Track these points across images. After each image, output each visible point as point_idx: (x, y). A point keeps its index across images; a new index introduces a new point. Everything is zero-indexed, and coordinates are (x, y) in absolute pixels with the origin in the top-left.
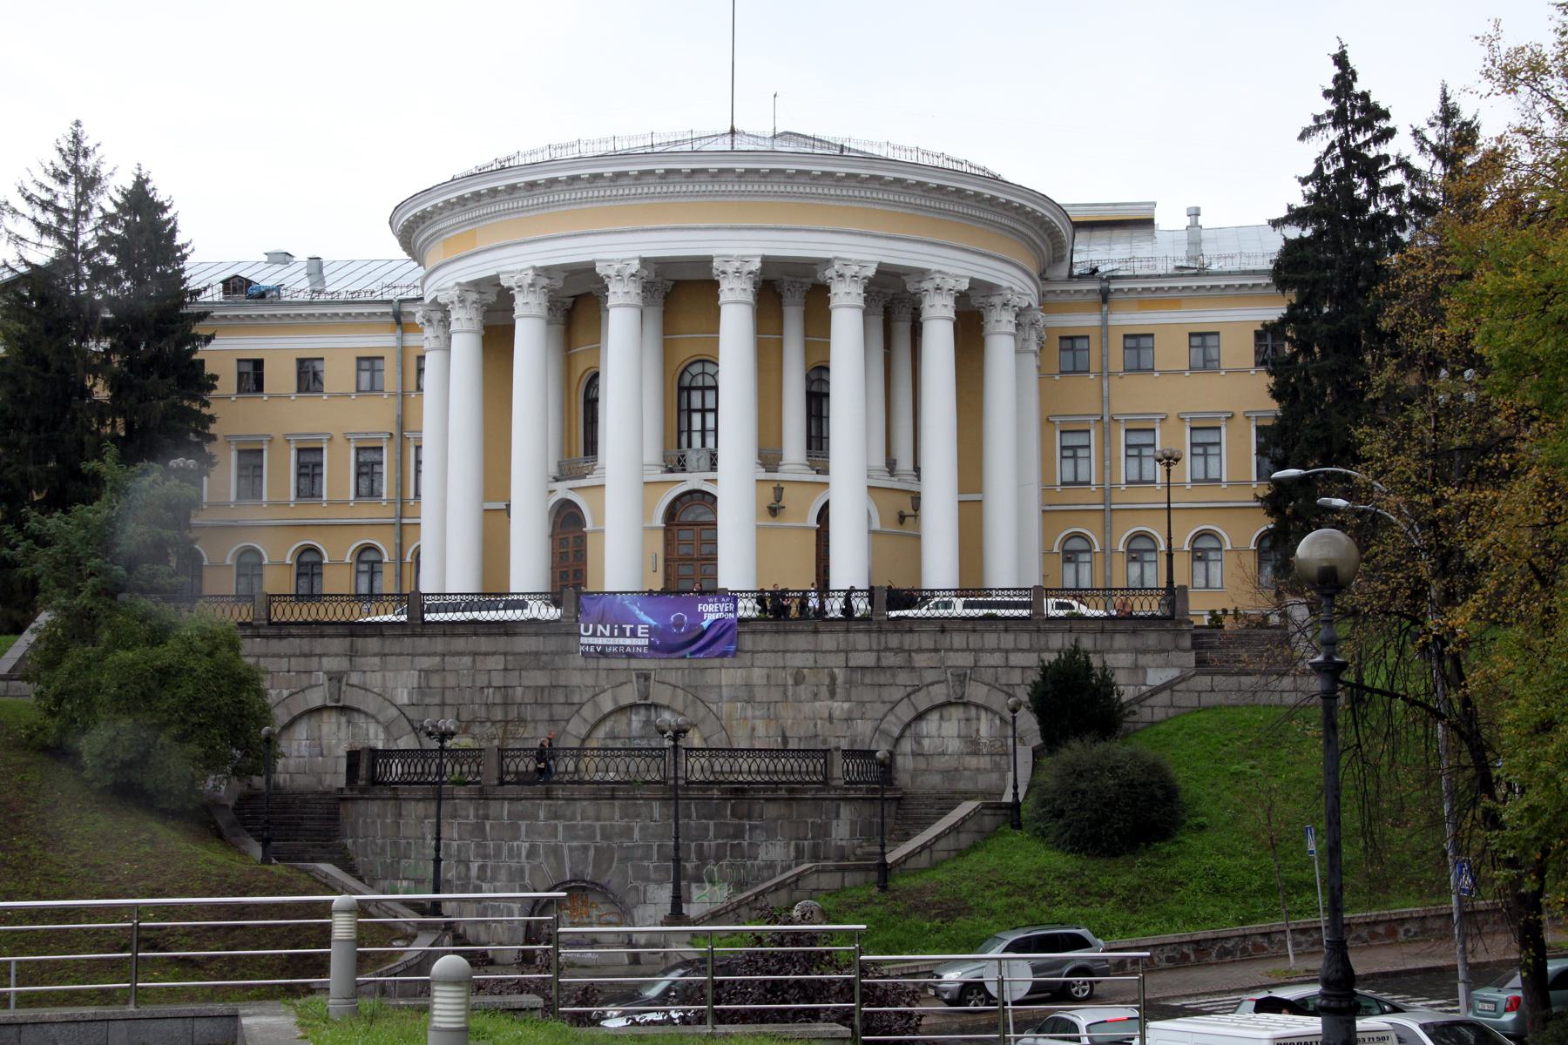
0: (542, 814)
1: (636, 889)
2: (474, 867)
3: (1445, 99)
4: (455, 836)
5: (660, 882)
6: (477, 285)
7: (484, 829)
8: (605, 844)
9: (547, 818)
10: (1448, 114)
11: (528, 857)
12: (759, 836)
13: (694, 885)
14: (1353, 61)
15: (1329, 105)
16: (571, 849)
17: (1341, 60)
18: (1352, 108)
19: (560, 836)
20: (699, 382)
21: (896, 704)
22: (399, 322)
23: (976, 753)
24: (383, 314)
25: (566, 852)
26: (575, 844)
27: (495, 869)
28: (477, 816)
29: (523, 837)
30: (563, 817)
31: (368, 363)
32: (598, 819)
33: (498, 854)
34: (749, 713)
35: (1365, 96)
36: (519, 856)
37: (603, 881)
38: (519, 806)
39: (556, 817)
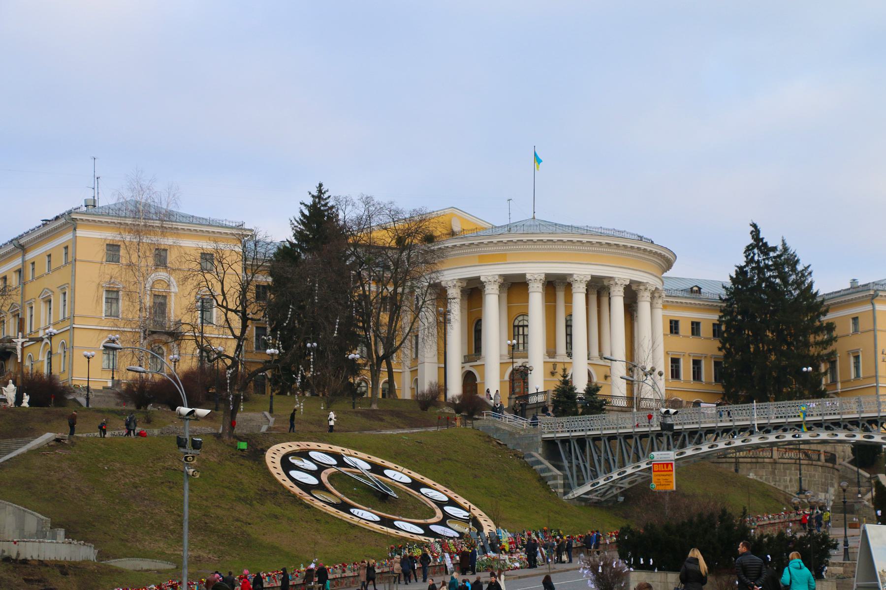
3: (784, 244)
6: (500, 276)
15: (752, 241)
17: (754, 226)
18: (758, 243)
35: (762, 239)
38: (786, 466)
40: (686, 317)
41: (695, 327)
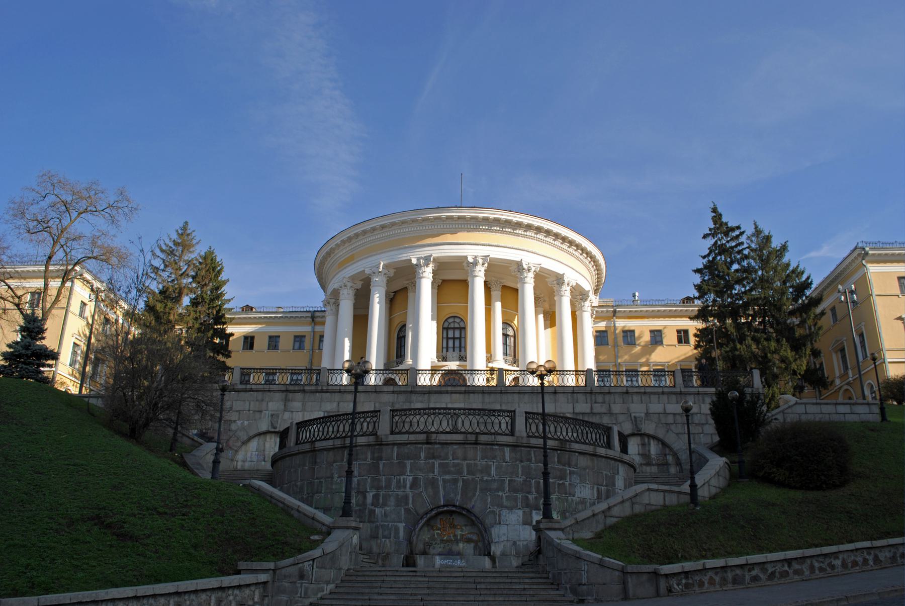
0: (423, 455)
5: (511, 509)
6: (353, 278)
7: (379, 467)
8: (470, 478)
9: (426, 458)
10: (758, 232)
11: (411, 488)
12: (576, 479)
13: (534, 512)
14: (720, 210)
16: (444, 481)
17: (714, 210)
20: (452, 325)
22: (313, 320)
23: (649, 464)
24: (307, 317)
25: (441, 483)
26: (447, 477)
27: (386, 498)
28: (373, 458)
30: (439, 457)
31: (299, 339)
32: (465, 459)
33: (388, 486)
36: (405, 487)
37: (469, 506)
38: (406, 450)
39: (434, 458)
40: (671, 326)
41: (683, 336)
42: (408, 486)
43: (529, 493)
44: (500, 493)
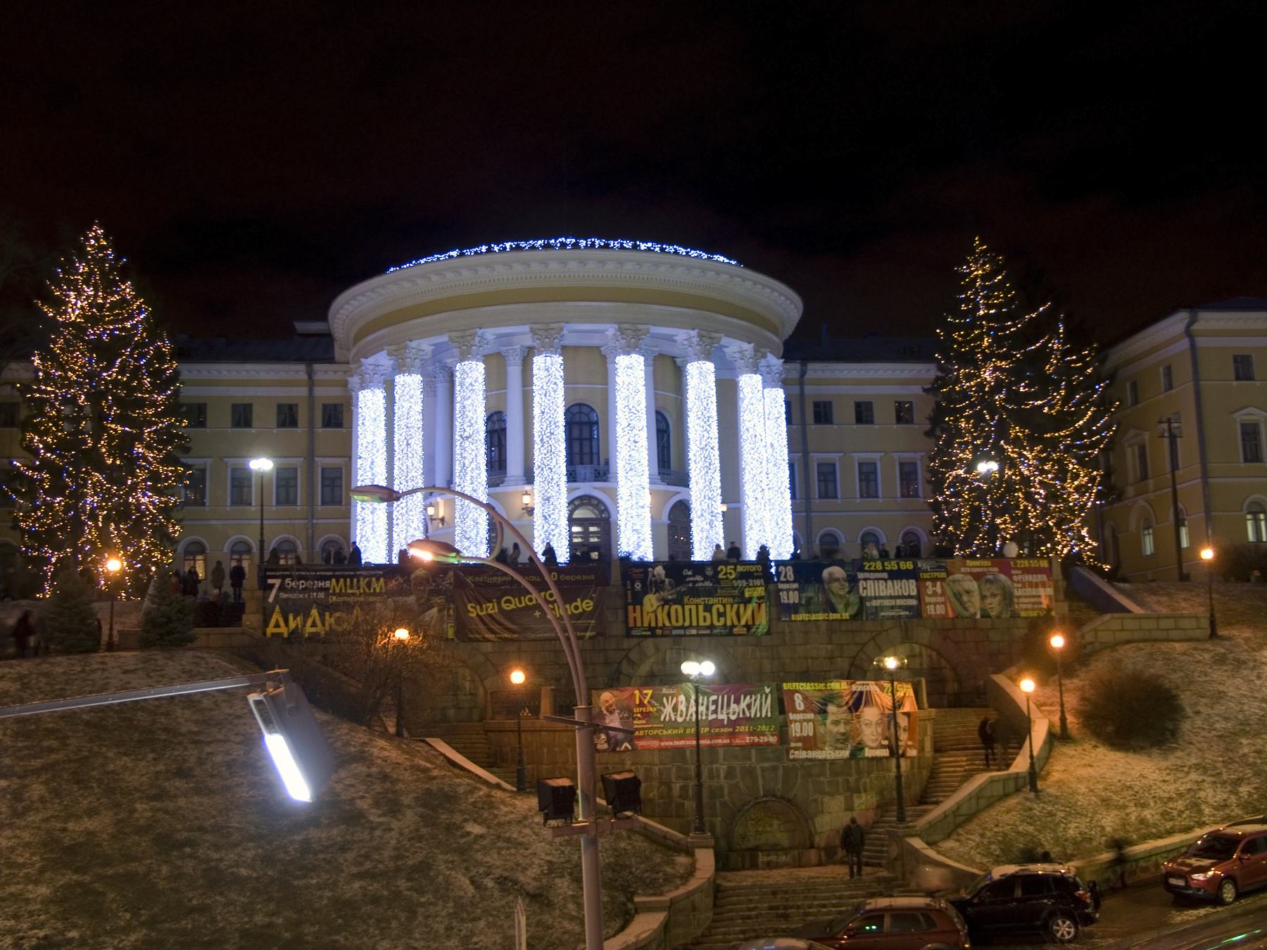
1: (816, 800)
2: (677, 787)
4: (656, 761)
5: (832, 795)
11: (726, 778)
16: (763, 770)
19: (753, 758)
21: (864, 645)
25: (759, 772)
26: (766, 765)
29: (721, 761)
34: (758, 653)
36: (718, 777)
37: (791, 795)
42: (722, 775)
43: (849, 775)
44: (822, 779)
